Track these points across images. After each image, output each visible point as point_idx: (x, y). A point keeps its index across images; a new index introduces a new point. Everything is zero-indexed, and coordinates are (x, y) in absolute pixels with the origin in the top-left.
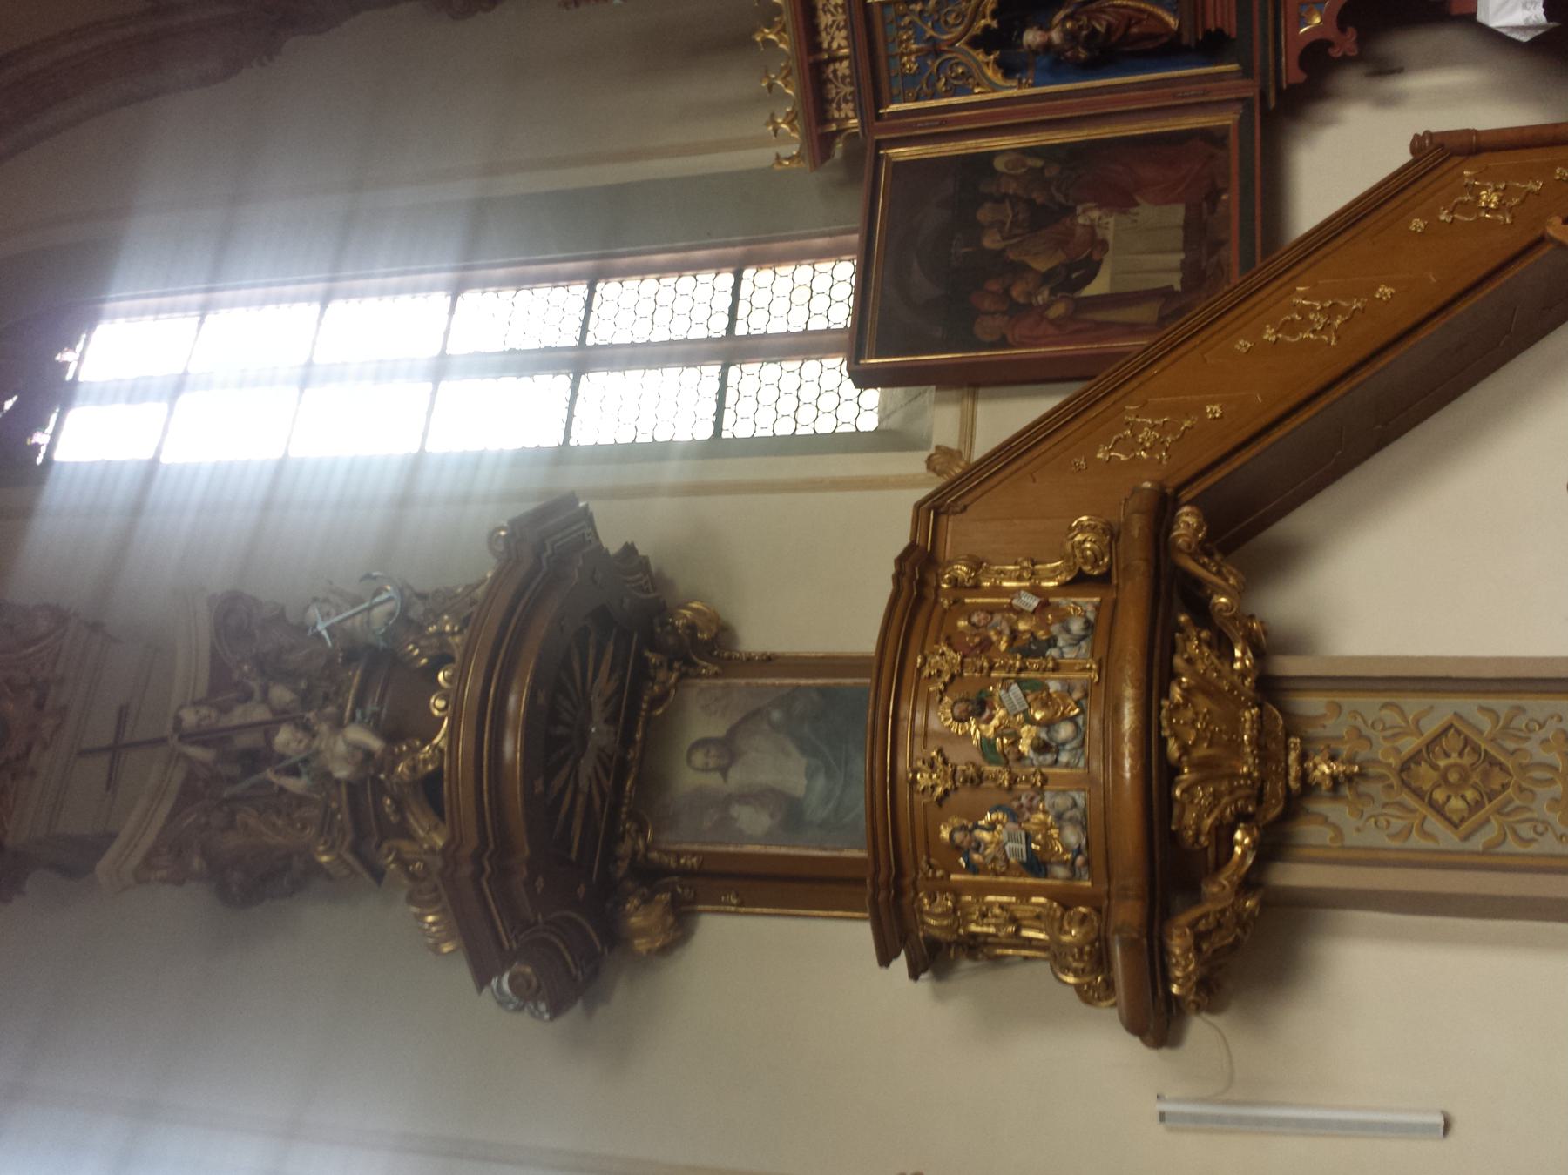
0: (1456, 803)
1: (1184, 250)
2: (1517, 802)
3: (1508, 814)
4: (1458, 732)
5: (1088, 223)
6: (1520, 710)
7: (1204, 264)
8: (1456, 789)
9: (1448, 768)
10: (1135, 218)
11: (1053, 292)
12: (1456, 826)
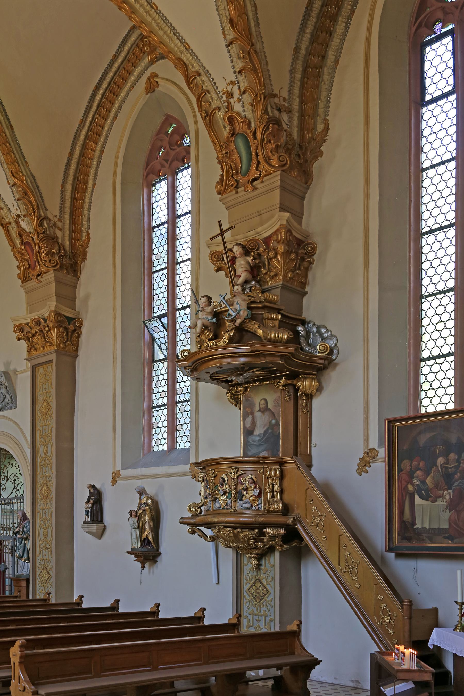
0: (253, 591)
1: (430, 529)
2: (253, 603)
3: (251, 601)
4: (267, 593)
5: (444, 495)
6: (272, 607)
7: (424, 535)
8: (256, 591)
9: (260, 590)
10: (445, 511)
11: (417, 485)
12: (248, 590)
